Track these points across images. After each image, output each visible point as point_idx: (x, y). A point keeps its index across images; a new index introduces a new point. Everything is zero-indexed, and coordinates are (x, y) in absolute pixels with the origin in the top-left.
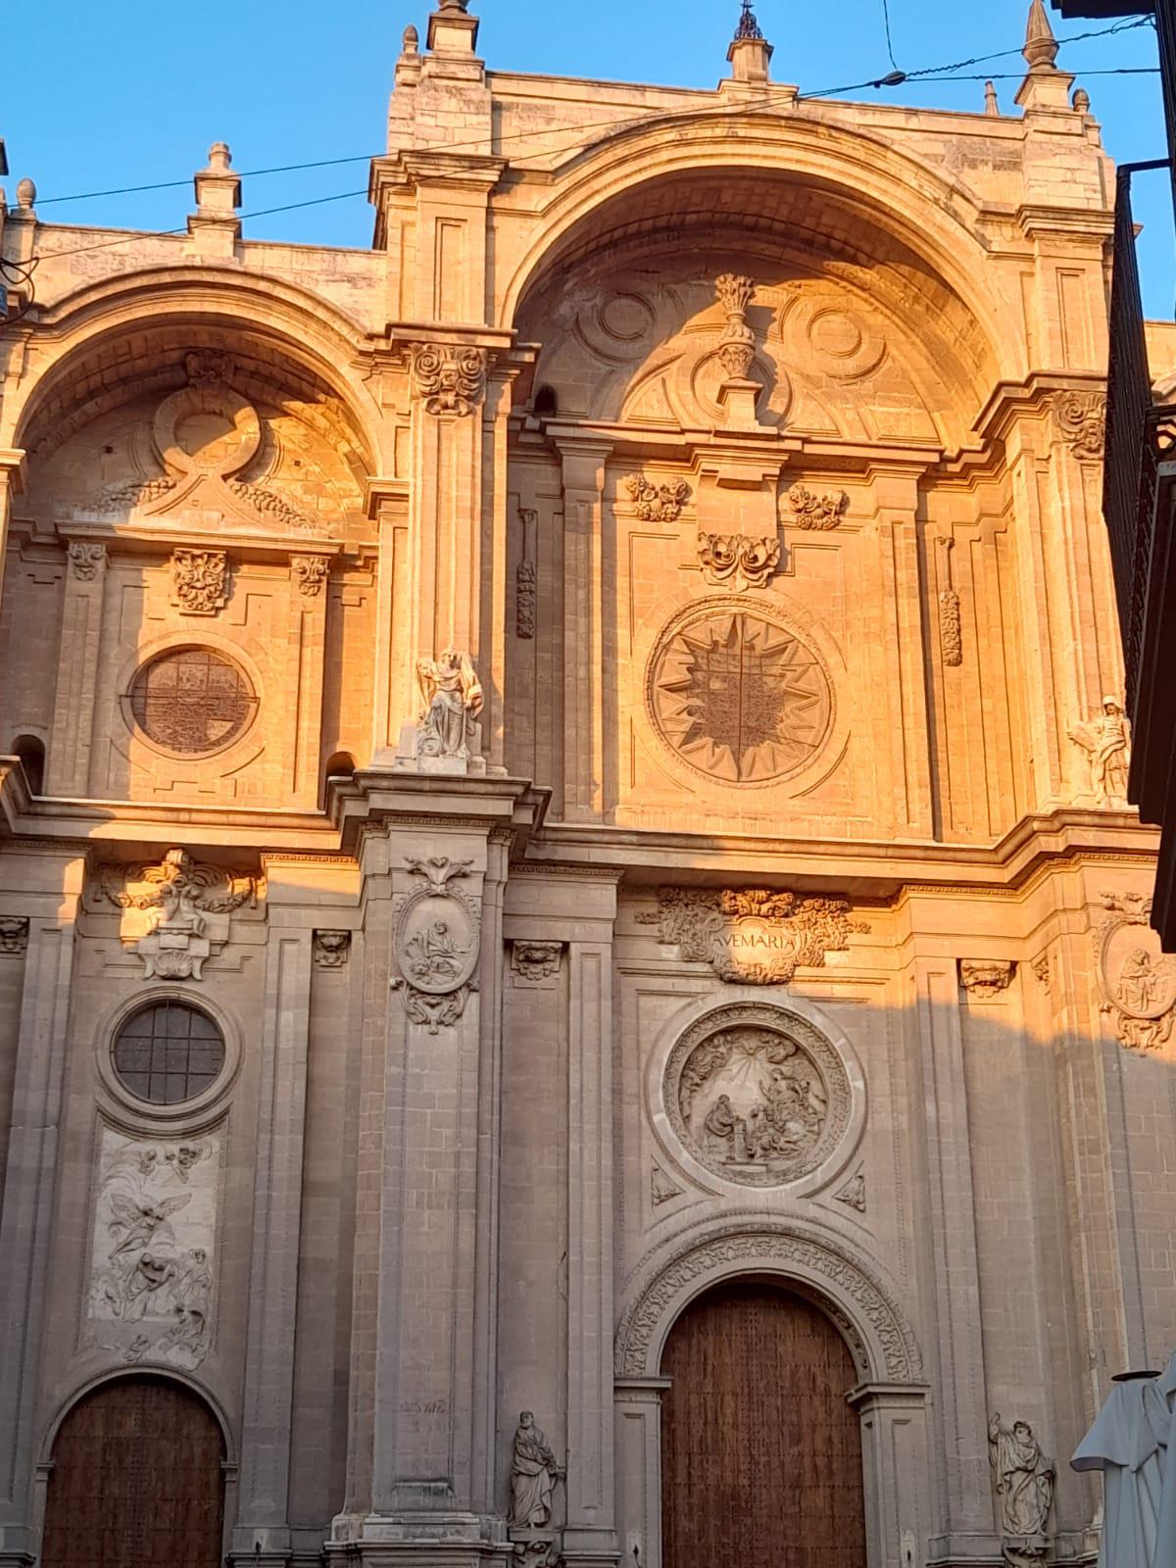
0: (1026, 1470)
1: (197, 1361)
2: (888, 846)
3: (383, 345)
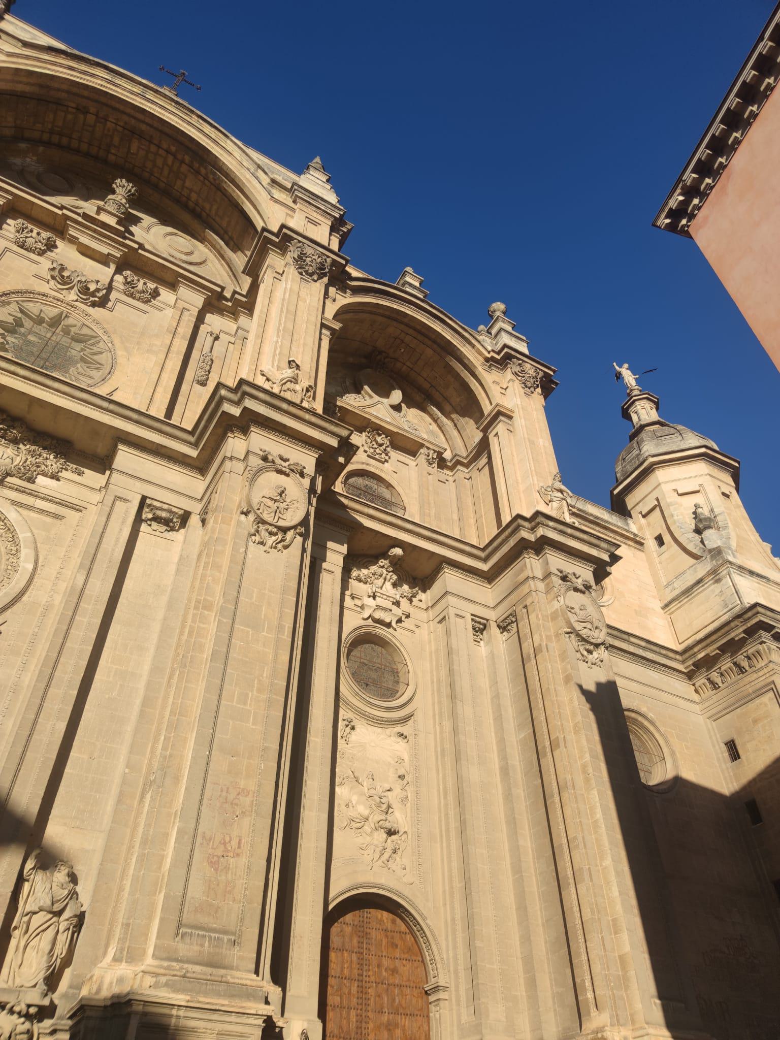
0: (50, 912)
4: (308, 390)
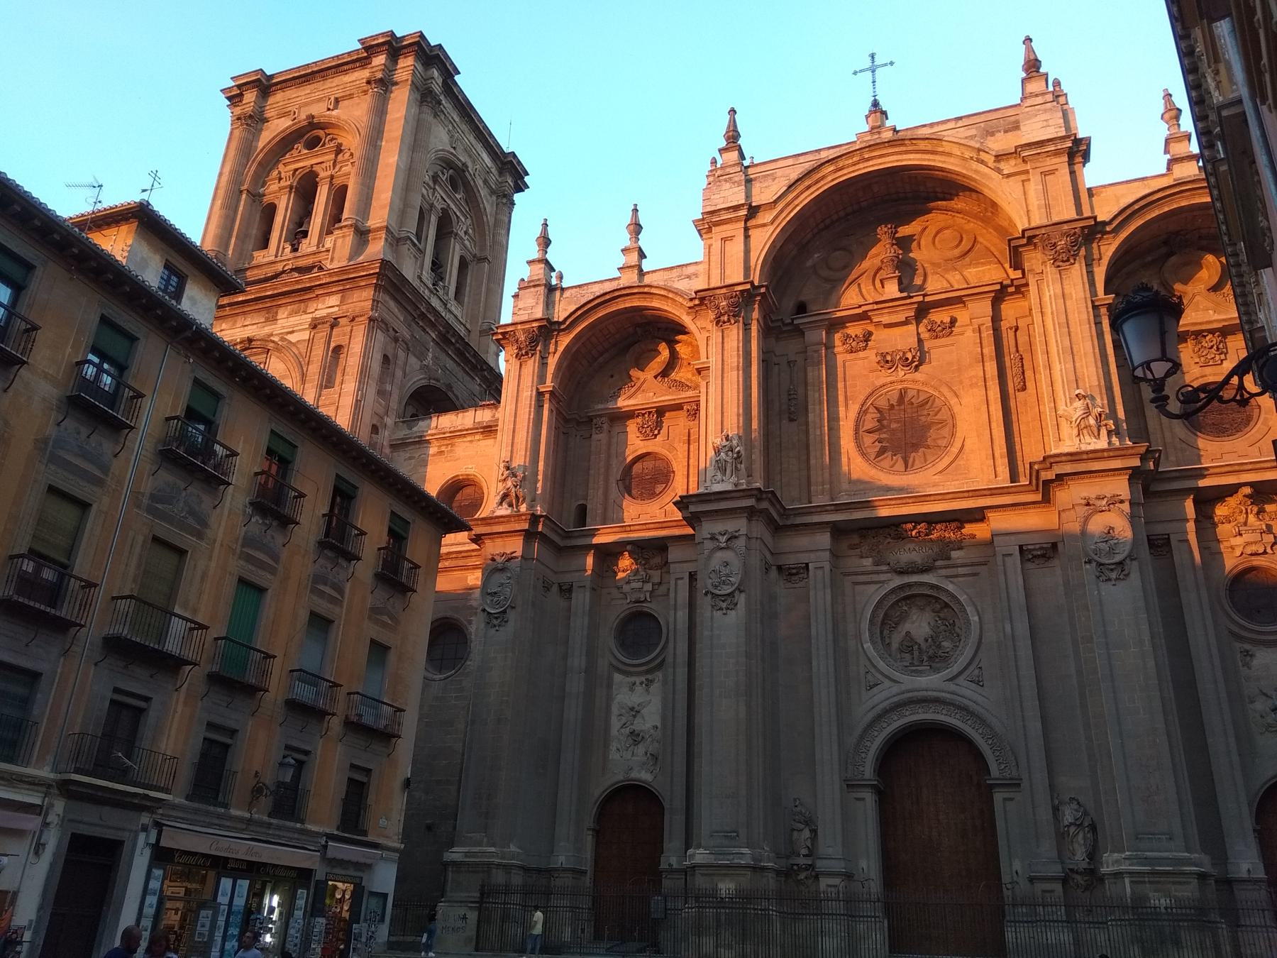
2: (968, 491)
3: (697, 302)
4: (1100, 415)
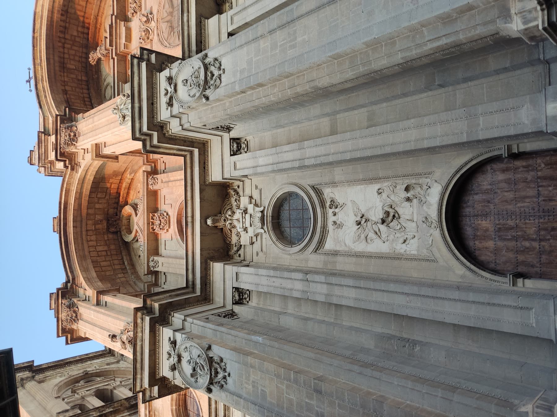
1: (436, 184)
